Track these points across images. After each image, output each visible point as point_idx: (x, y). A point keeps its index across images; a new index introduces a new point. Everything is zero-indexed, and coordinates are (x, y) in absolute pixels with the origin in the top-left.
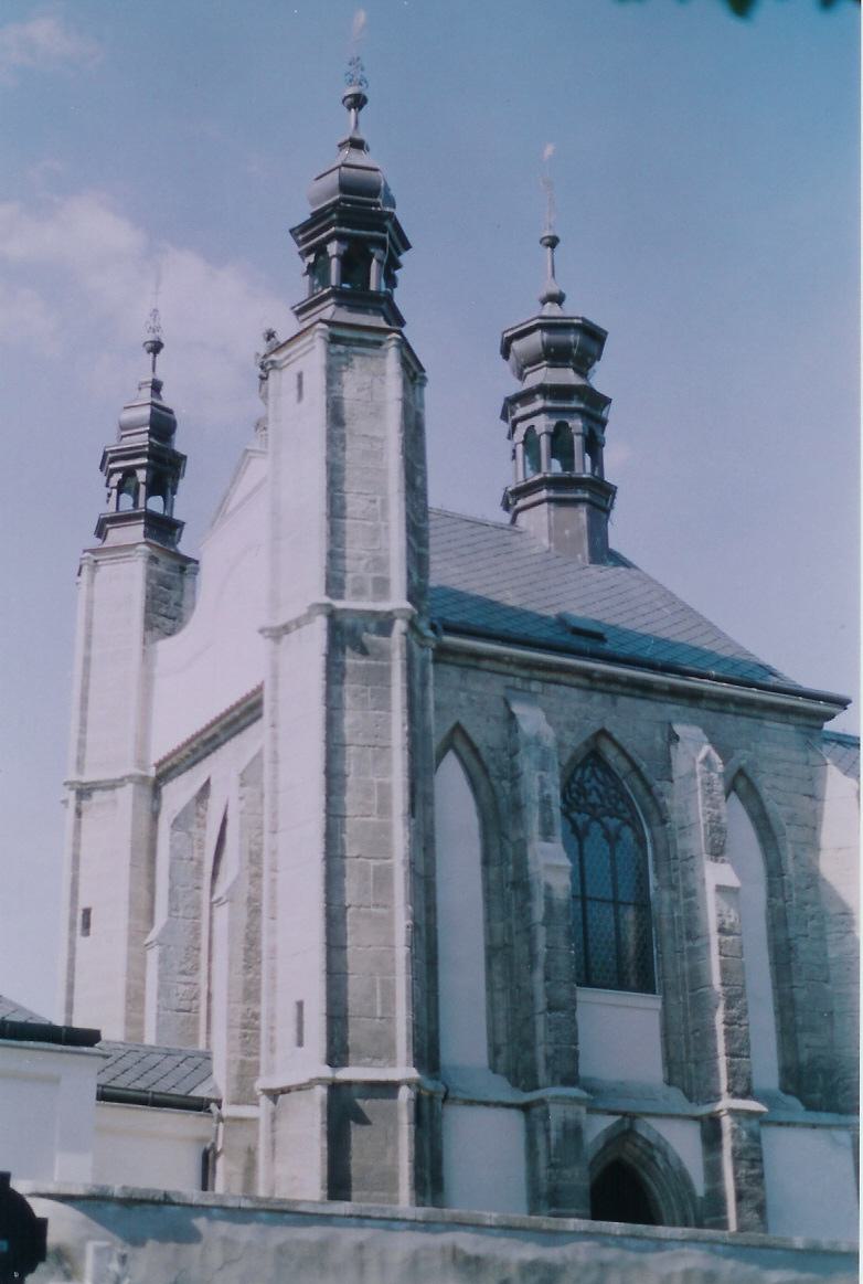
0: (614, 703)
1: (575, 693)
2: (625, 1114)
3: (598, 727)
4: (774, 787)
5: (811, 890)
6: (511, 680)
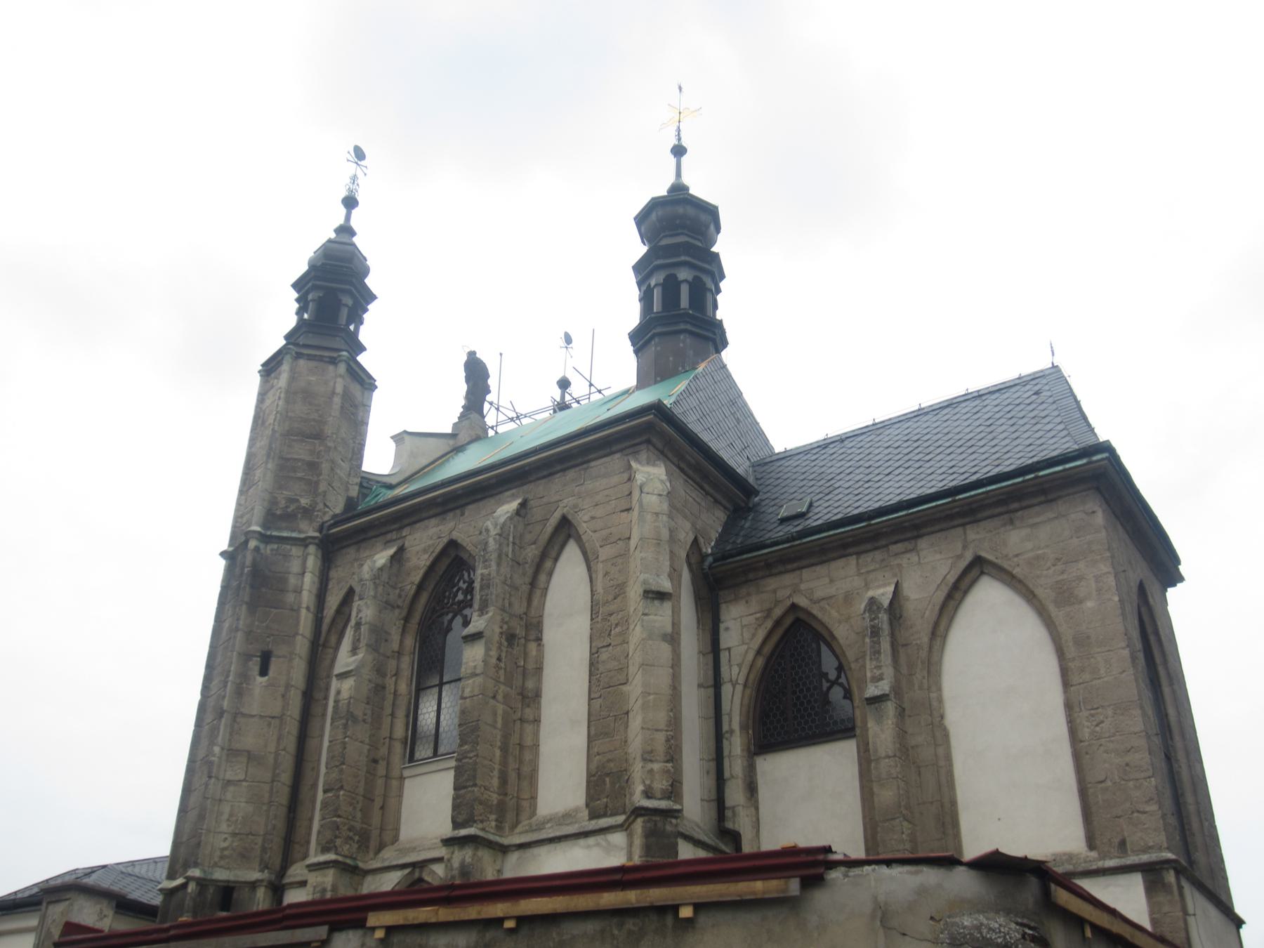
0: (463, 514)
1: (433, 521)
2: (413, 865)
3: (445, 540)
4: (593, 518)
5: (619, 599)
6: (389, 536)
